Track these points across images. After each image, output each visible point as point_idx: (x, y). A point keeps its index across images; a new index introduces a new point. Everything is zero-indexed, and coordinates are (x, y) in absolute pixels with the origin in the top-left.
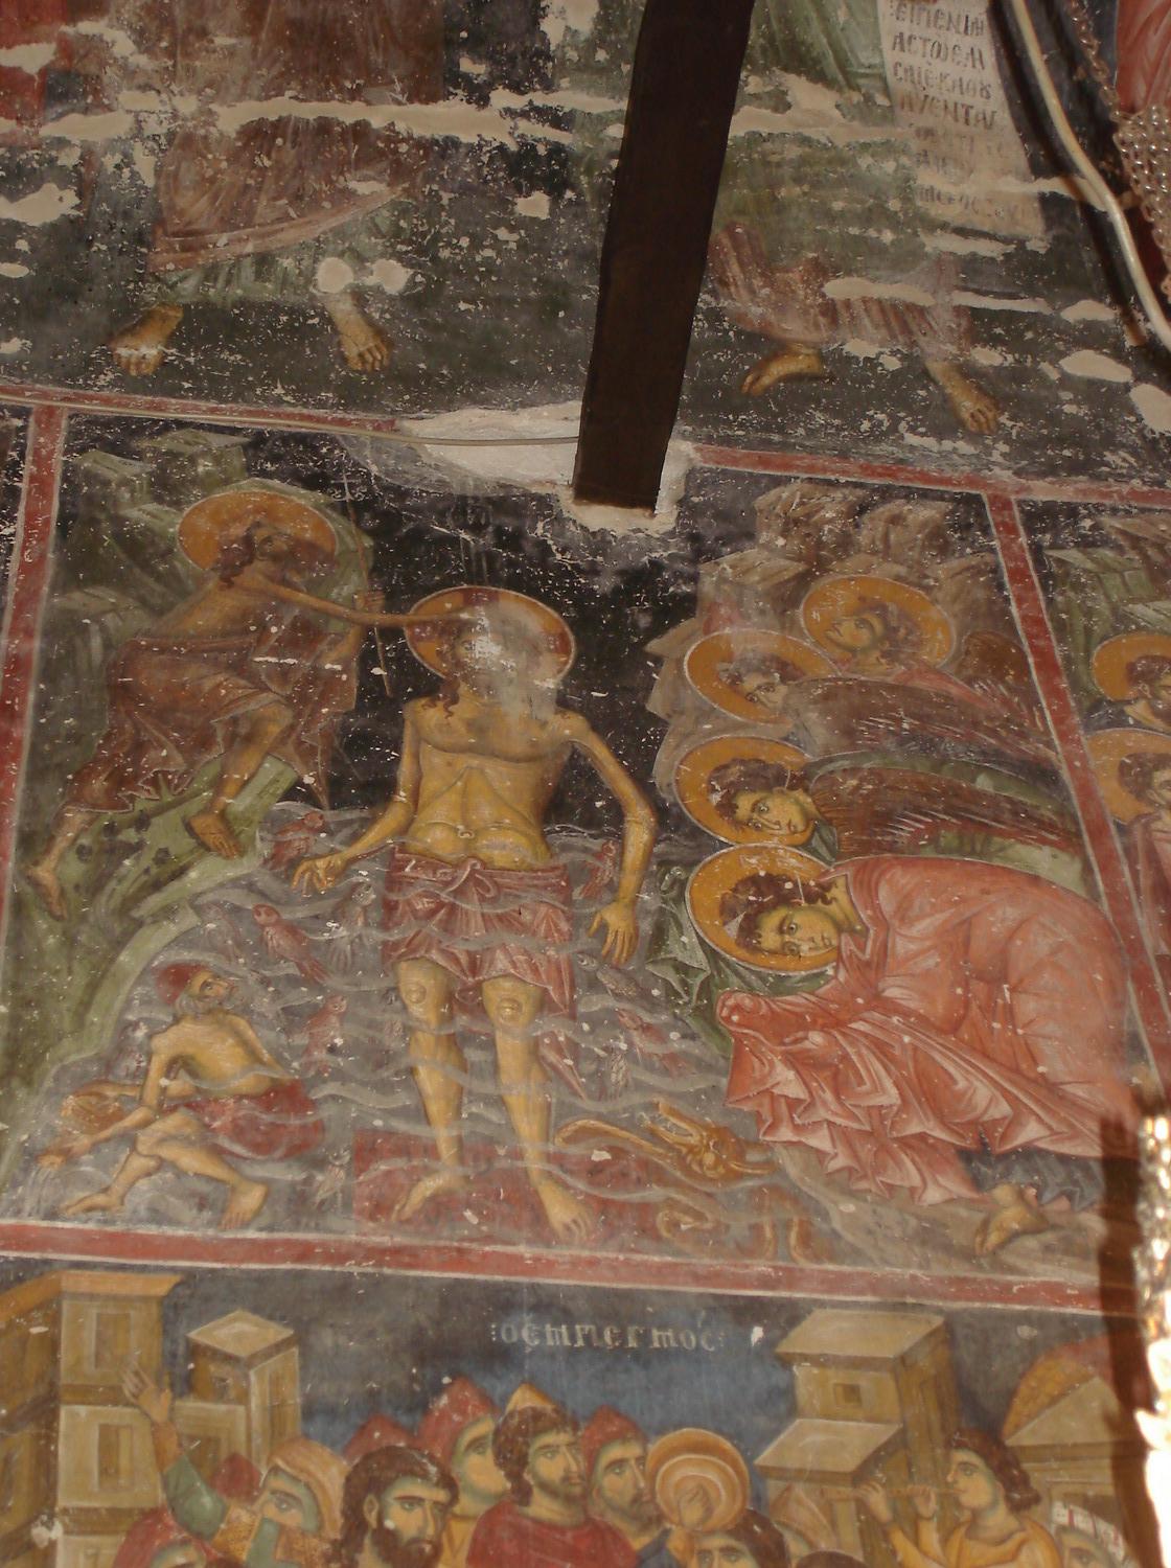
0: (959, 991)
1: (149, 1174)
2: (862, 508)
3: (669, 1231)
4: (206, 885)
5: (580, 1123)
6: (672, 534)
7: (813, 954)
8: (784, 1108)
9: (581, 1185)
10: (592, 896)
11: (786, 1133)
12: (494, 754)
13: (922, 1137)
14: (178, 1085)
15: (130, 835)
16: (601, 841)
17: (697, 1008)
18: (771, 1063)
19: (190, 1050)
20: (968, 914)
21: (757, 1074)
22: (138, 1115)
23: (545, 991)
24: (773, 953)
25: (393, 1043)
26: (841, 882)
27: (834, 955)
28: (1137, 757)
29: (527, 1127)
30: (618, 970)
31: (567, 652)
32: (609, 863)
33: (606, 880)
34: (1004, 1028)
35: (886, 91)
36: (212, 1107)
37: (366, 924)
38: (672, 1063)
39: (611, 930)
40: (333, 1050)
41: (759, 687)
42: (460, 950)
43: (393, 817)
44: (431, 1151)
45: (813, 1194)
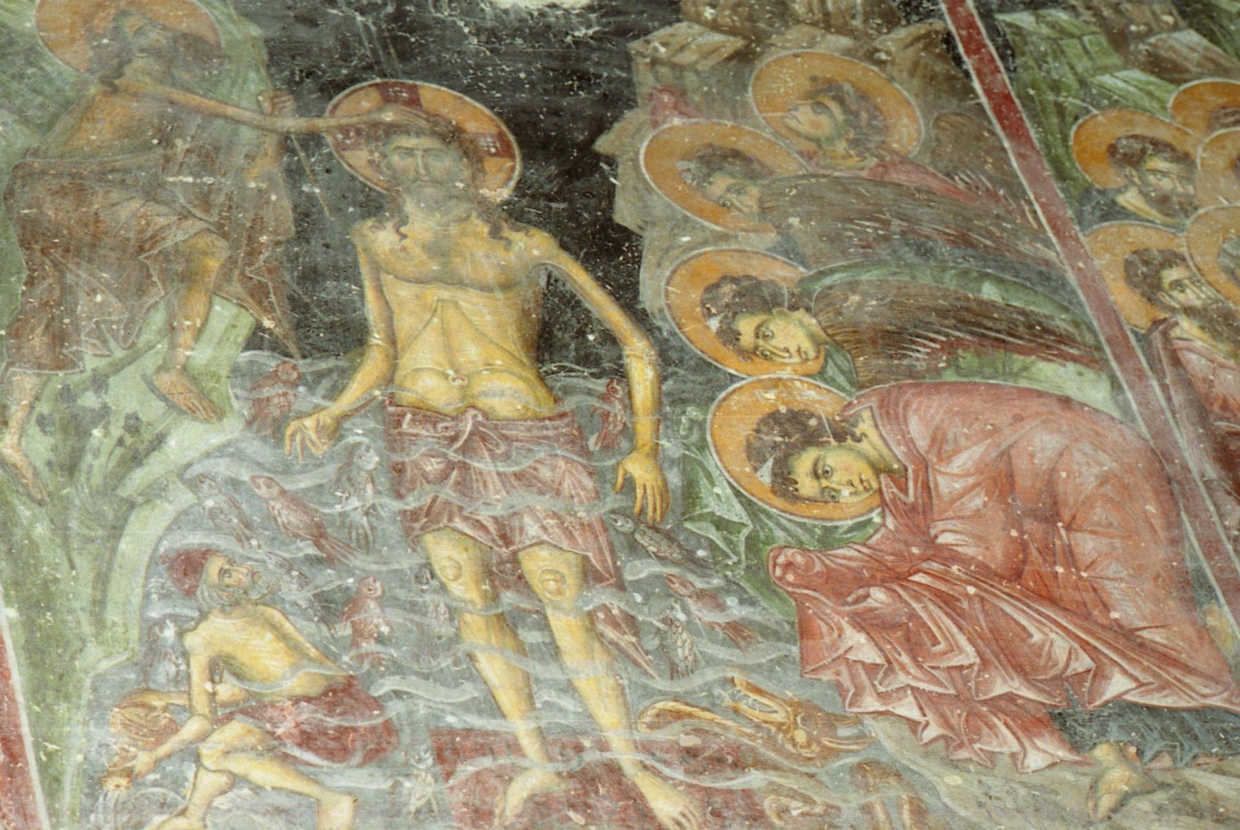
0: (1014, 533)
1: (223, 792)
3: (780, 818)
4: (191, 455)
5: (660, 705)
7: (855, 499)
8: (864, 677)
9: (678, 774)
10: (608, 447)
11: (871, 703)
12: (461, 284)
13: (1011, 697)
14: (227, 690)
15: (89, 400)
16: (604, 381)
17: (748, 567)
18: (841, 629)
19: (228, 649)
20: (1004, 445)
21: (827, 640)
23: (586, 558)
24: (812, 500)
26: (866, 414)
27: (877, 500)
28: (1142, 254)
29: (608, 716)
30: (657, 530)
31: (512, 157)
32: (618, 406)
33: (620, 427)
34: (1069, 573)
36: (270, 712)
37: (378, 493)
38: (737, 632)
39: (639, 483)
40: (380, 640)
41: (728, 190)
42: (484, 516)
43: (371, 367)
44: (514, 747)
45: (914, 767)
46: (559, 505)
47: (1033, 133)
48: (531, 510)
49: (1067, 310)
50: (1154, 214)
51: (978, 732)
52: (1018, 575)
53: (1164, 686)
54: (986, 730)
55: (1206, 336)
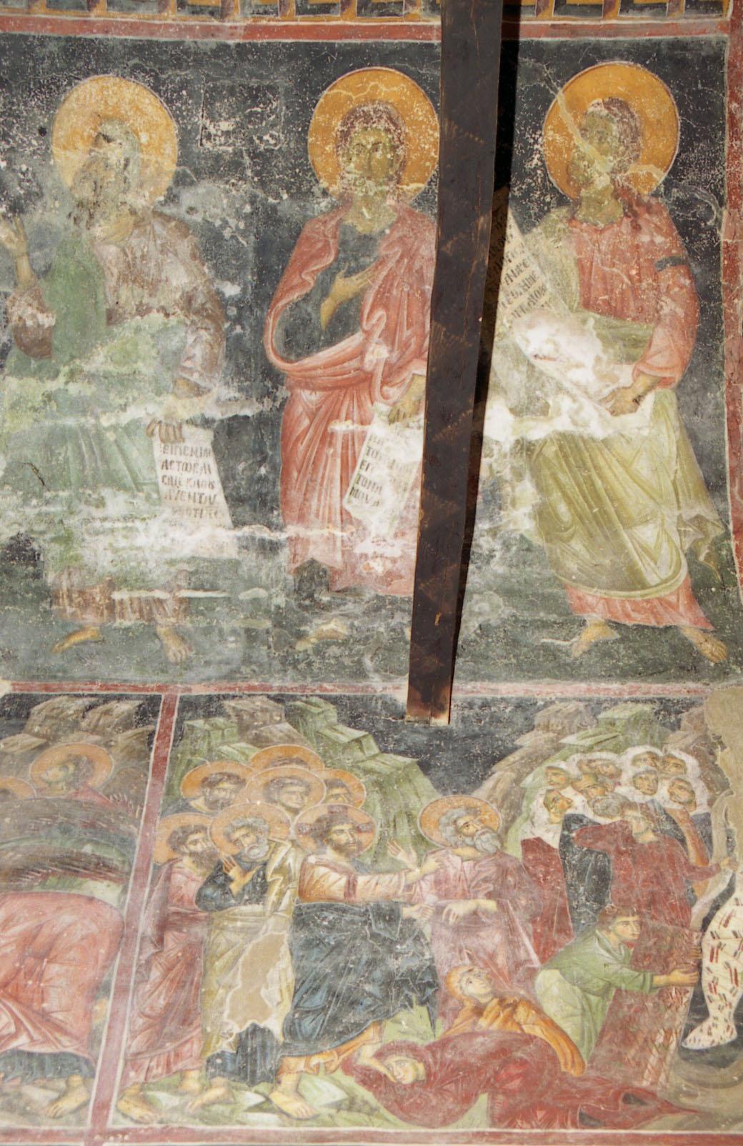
2: (91, 707)
35: (158, 492)
47: (166, 775)
49: (123, 855)
55: (193, 866)
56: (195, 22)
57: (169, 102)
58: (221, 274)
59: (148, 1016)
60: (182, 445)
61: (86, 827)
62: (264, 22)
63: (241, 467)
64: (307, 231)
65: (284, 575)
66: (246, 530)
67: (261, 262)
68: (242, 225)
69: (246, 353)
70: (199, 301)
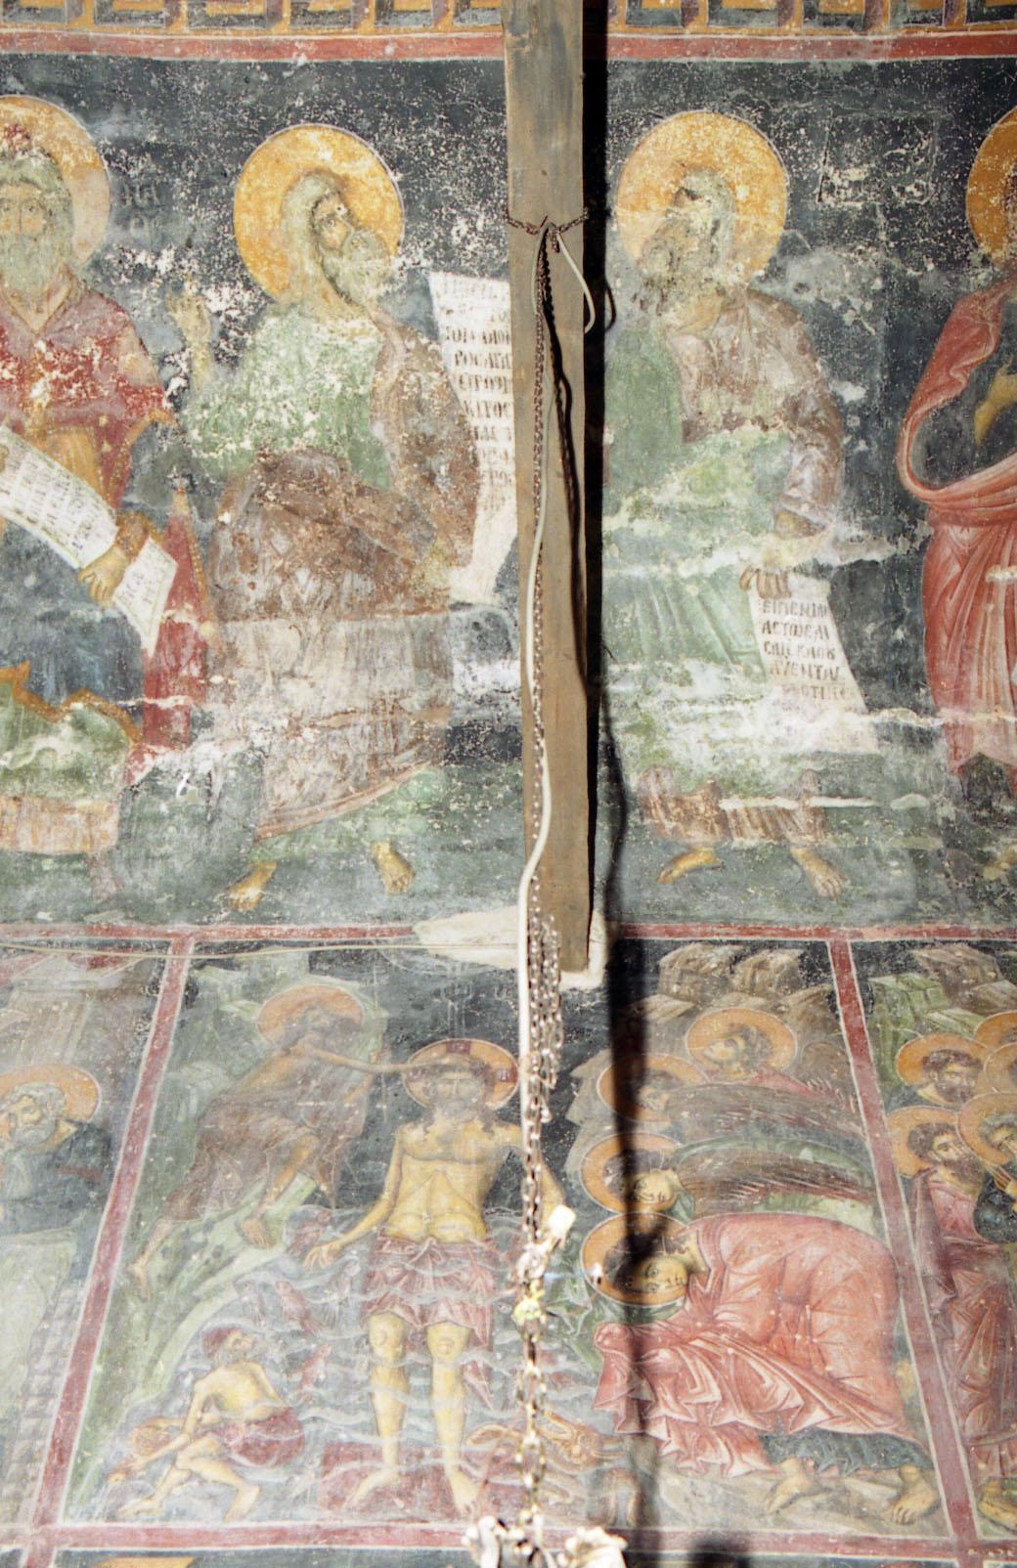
2: (737, 959)
6: (598, 990)
12: (453, 1160)
13: (735, 1425)
22: (180, 1440)
25: (359, 1375)
26: (693, 1236)
28: (925, 1128)
35: (760, 664)
36: (232, 1431)
38: (559, 1379)
40: (317, 1384)
44: (377, 1455)
46: (466, 1298)
47: (871, 1053)
48: (446, 1300)
49: (856, 1164)
50: (942, 1101)
51: (704, 1448)
52: (767, 1340)
53: (850, 1418)
54: (709, 1447)
55: (955, 1179)
56: (825, 36)
57: (780, 144)
58: (839, 372)
59: (974, 1387)
60: (788, 601)
61: (791, 1124)
62: (921, 34)
63: (869, 629)
64: (958, 313)
65: (945, 776)
66: (885, 715)
67: (894, 356)
68: (869, 306)
69: (872, 476)
70: (808, 409)
